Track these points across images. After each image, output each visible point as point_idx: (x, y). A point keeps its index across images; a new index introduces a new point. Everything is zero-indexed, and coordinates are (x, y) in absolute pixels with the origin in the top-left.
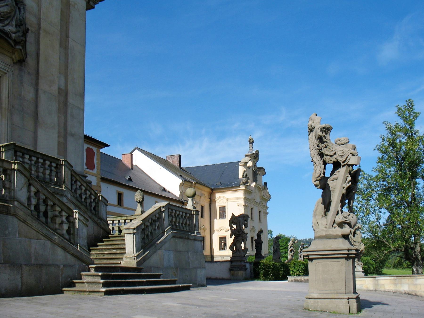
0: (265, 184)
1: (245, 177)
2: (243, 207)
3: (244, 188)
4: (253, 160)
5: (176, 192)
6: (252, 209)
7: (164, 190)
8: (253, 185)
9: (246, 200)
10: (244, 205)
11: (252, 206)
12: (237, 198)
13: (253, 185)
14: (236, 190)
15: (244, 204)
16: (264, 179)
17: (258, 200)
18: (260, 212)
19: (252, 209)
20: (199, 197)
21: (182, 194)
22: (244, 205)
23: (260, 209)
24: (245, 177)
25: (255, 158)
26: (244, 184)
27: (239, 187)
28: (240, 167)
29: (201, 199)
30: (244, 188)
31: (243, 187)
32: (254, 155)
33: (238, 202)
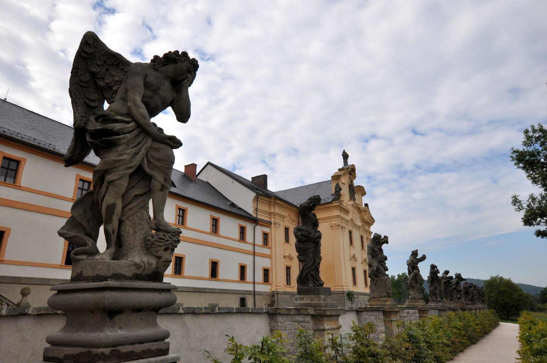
0: (366, 205)
5: (250, 210)
6: (350, 232)
7: (233, 205)
11: (351, 228)
12: (330, 218)
16: (365, 200)
18: (362, 237)
19: (350, 232)
21: (256, 210)
25: (350, 174)
32: (350, 170)
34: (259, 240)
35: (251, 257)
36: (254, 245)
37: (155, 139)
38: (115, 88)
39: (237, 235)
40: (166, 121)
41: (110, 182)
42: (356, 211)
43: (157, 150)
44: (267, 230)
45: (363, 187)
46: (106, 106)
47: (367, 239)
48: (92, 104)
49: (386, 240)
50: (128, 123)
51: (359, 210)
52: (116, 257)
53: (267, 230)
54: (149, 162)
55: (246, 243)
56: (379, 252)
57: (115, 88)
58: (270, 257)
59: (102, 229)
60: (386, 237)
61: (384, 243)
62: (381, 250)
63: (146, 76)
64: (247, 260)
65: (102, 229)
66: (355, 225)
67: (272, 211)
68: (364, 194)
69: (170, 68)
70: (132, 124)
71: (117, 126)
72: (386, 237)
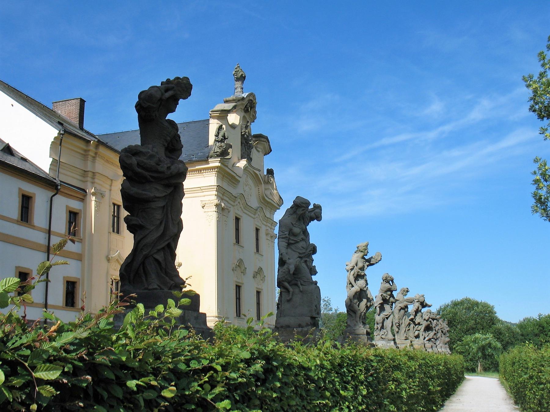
0: (270, 172)
1: (222, 141)
2: (214, 209)
3: (219, 164)
4: (243, 114)
5: (43, 162)
6: (237, 220)
8: (243, 163)
9: (221, 192)
10: (217, 205)
11: (240, 213)
12: (201, 189)
13: (243, 163)
14: (200, 171)
15: (216, 202)
17: (254, 203)
18: (257, 230)
19: (237, 220)
20: (109, 182)
21: (56, 164)
22: (217, 205)
23: (259, 224)
24: (222, 141)
26: (218, 156)
27: (206, 161)
28: (212, 121)
29: (113, 188)
30: (219, 164)
31: (215, 163)
33: (203, 199)
34: (60, 224)
35: (40, 257)
36: (49, 232)
39: (15, 212)
42: (250, 182)
44: (75, 205)
45: (267, 138)
47: (267, 234)
49: (316, 214)
51: (256, 179)
53: (75, 205)
55: (33, 227)
56: (302, 236)
58: (79, 257)
60: (318, 208)
61: (312, 219)
62: (306, 233)
64: (33, 261)
66: (247, 206)
67: (89, 168)
68: (269, 151)
72: (318, 208)
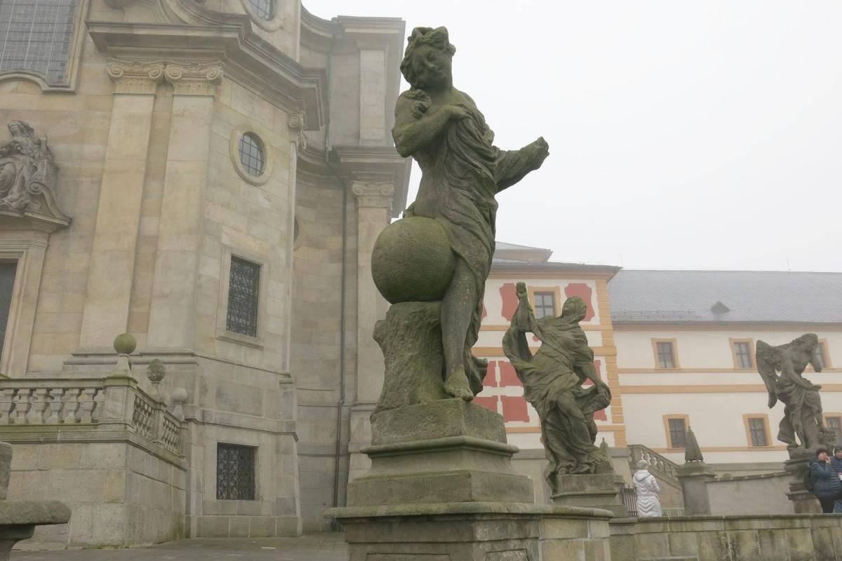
37: (807, 389)
38: (779, 364)
40: (810, 376)
41: (793, 415)
43: (809, 394)
46: (779, 374)
48: (770, 375)
50: (791, 385)
52: (807, 446)
54: (808, 401)
57: (779, 364)
59: (795, 433)
63: (792, 358)
65: (795, 433)
69: (803, 346)
70: (794, 385)
71: (787, 389)
